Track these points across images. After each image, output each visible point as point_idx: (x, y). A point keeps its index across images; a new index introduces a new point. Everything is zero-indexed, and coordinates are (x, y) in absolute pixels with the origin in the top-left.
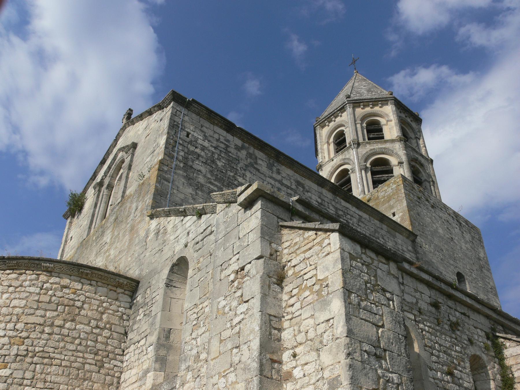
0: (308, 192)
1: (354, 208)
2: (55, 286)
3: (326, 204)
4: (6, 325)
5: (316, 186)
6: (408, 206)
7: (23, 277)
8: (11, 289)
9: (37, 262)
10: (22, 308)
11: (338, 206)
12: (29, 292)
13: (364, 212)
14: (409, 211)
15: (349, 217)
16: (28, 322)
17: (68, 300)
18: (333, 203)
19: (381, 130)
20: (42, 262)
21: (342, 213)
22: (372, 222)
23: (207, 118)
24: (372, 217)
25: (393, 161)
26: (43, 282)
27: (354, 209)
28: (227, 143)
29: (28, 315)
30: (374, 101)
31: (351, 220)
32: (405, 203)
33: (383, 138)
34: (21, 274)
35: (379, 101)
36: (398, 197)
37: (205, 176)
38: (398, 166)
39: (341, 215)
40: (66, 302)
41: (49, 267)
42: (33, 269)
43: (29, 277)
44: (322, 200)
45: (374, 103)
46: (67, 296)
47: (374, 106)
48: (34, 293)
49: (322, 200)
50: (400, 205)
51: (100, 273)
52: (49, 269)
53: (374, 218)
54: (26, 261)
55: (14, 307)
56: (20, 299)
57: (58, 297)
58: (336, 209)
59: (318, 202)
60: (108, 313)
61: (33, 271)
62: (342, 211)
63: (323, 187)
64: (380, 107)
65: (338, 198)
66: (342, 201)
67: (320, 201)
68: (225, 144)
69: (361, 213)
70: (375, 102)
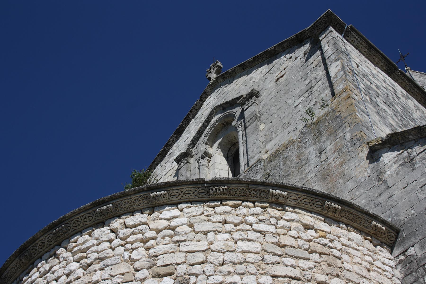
2: (294, 225)
4: (242, 279)
7: (242, 210)
8: (229, 227)
9: (260, 188)
10: (257, 253)
12: (260, 232)
16: (277, 273)
17: (319, 245)
20: (268, 188)
23: (367, 54)
26: (276, 218)
28: (393, 87)
29: (273, 263)
34: (235, 207)
37: (392, 117)
40: (319, 248)
41: (280, 196)
42: (253, 199)
43: (252, 210)
46: (317, 240)
48: (268, 232)
51: (352, 211)
52: (281, 200)
54: (243, 187)
55: (243, 252)
56: (250, 240)
57: (305, 240)
60: (374, 271)
61: (254, 203)
68: (393, 88)
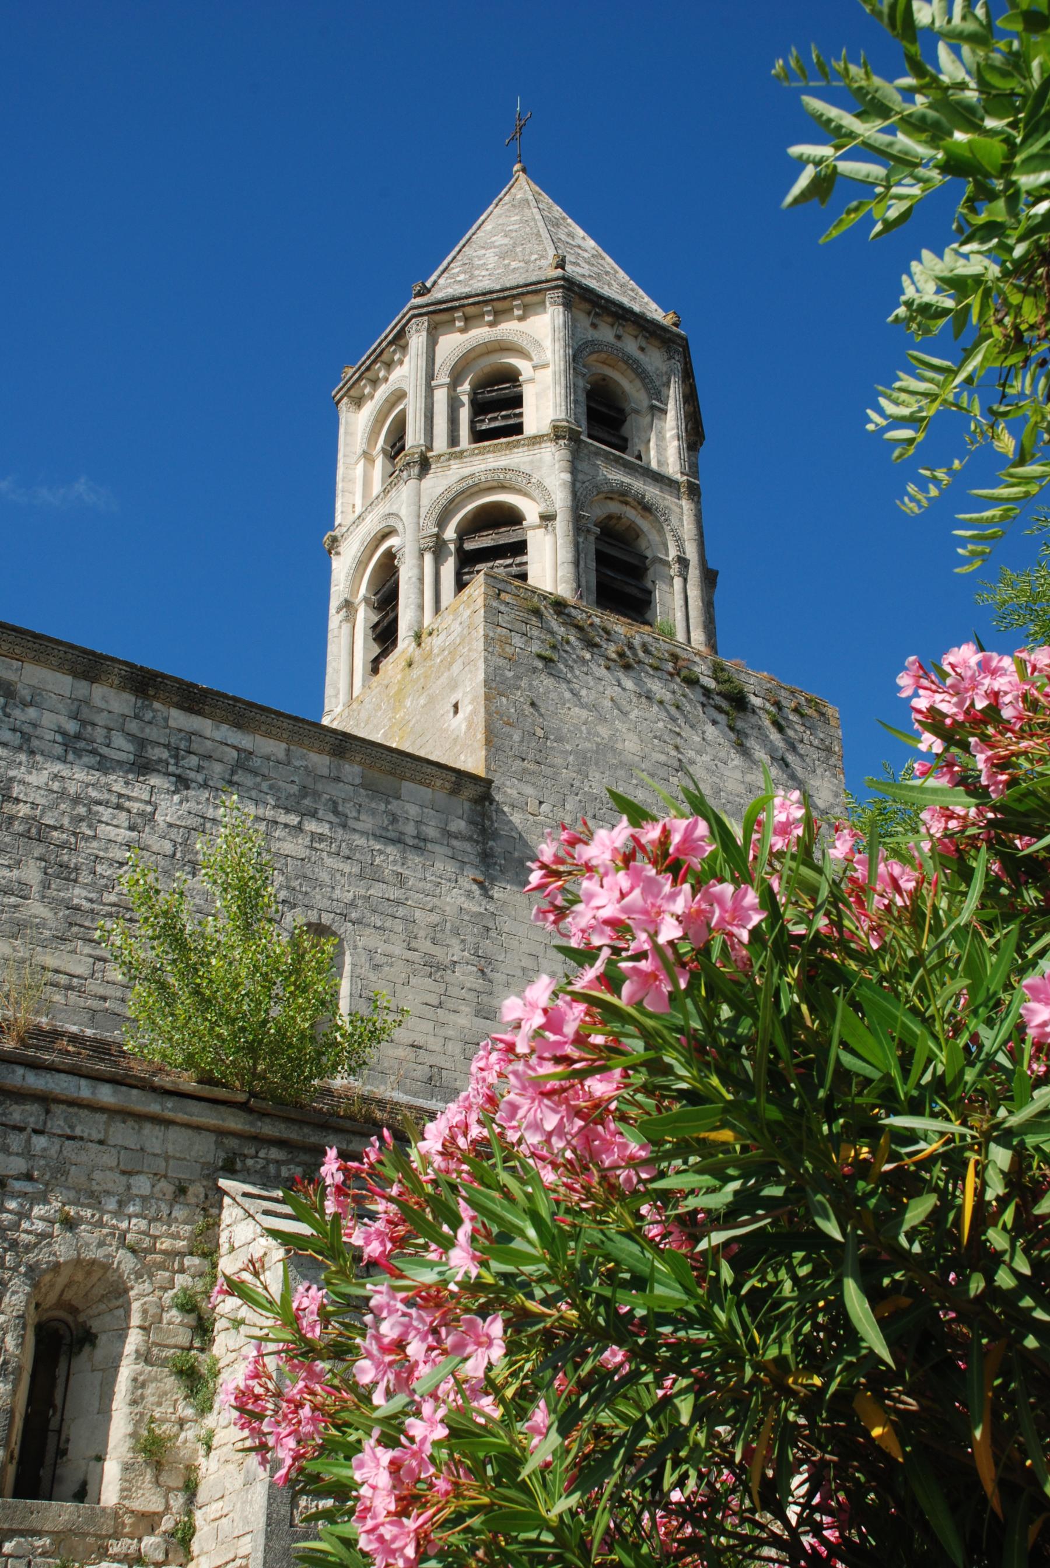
0: (25, 705)
1: (225, 727)
3: (99, 734)
5: (69, 679)
6: (487, 682)
11: (152, 733)
13: (268, 734)
14: (488, 698)
15: (193, 760)
18: (133, 726)
19: (517, 401)
21: (165, 755)
22: (297, 763)
24: (301, 744)
25: (530, 510)
27: (226, 733)
30: (498, 299)
31: (199, 769)
32: (481, 676)
33: (518, 429)
35: (514, 297)
36: (470, 650)
38: (539, 527)
39: (160, 761)
44: (84, 723)
45: (499, 305)
47: (500, 315)
49: (84, 723)
50: (471, 680)
53: (310, 748)
58: (142, 743)
59: (64, 734)
62: (167, 746)
63: (93, 680)
64: (521, 319)
65: (156, 705)
66: (174, 712)
67: (72, 727)
69: (245, 741)
70: (501, 302)
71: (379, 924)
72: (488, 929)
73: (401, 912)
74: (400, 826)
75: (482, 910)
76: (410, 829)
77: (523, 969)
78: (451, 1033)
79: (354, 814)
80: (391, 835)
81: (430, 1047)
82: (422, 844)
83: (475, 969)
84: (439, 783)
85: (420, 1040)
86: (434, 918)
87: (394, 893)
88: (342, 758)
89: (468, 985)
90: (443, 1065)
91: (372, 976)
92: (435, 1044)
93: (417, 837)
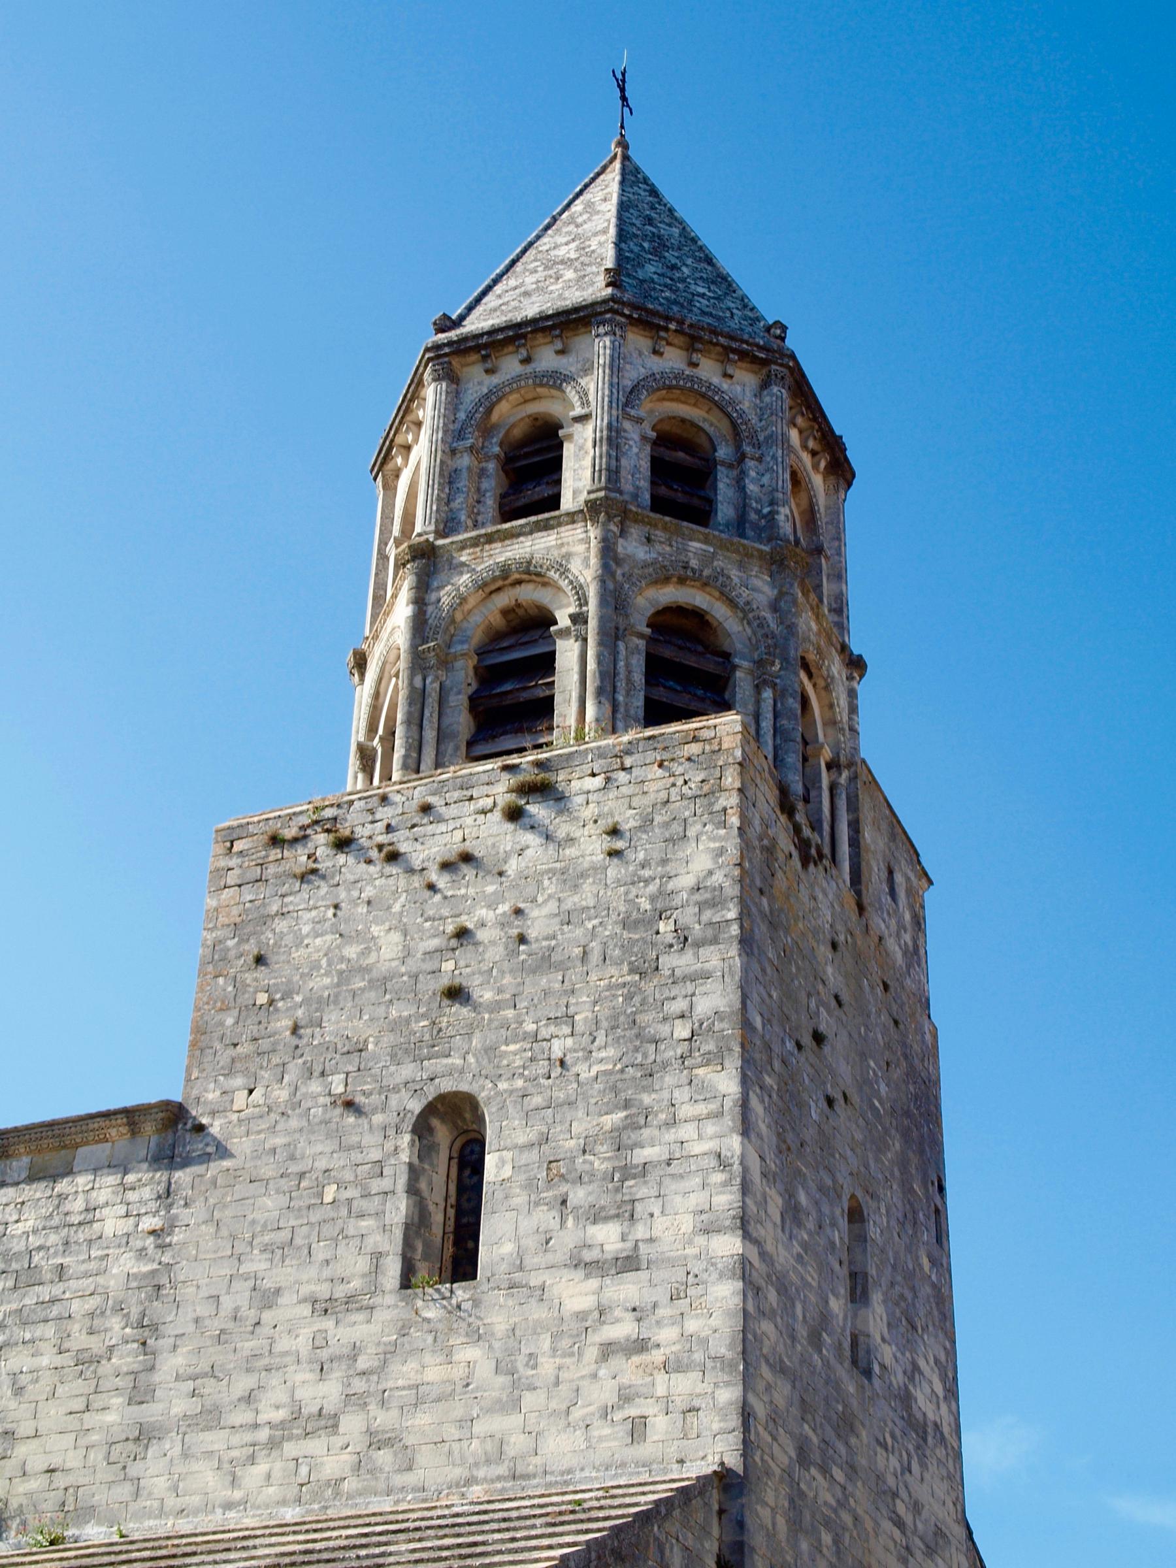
71: (28, 1336)
72: (159, 1288)
73: (55, 1311)
74: (67, 1206)
75: (155, 1266)
76: (79, 1204)
77: (197, 1321)
78: (94, 1437)
79: (15, 1217)
80: (56, 1221)
81: (68, 1465)
82: (90, 1216)
83: (135, 1345)
84: (113, 1132)
85: (56, 1461)
86: (92, 1303)
87: (45, 1292)
88: (8, 1157)
89: (125, 1369)
90: (81, 1481)
91: (13, 1404)
92: (73, 1460)
93: (87, 1210)
